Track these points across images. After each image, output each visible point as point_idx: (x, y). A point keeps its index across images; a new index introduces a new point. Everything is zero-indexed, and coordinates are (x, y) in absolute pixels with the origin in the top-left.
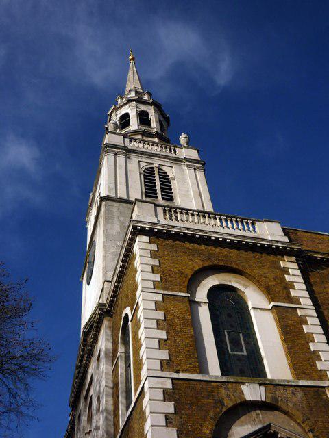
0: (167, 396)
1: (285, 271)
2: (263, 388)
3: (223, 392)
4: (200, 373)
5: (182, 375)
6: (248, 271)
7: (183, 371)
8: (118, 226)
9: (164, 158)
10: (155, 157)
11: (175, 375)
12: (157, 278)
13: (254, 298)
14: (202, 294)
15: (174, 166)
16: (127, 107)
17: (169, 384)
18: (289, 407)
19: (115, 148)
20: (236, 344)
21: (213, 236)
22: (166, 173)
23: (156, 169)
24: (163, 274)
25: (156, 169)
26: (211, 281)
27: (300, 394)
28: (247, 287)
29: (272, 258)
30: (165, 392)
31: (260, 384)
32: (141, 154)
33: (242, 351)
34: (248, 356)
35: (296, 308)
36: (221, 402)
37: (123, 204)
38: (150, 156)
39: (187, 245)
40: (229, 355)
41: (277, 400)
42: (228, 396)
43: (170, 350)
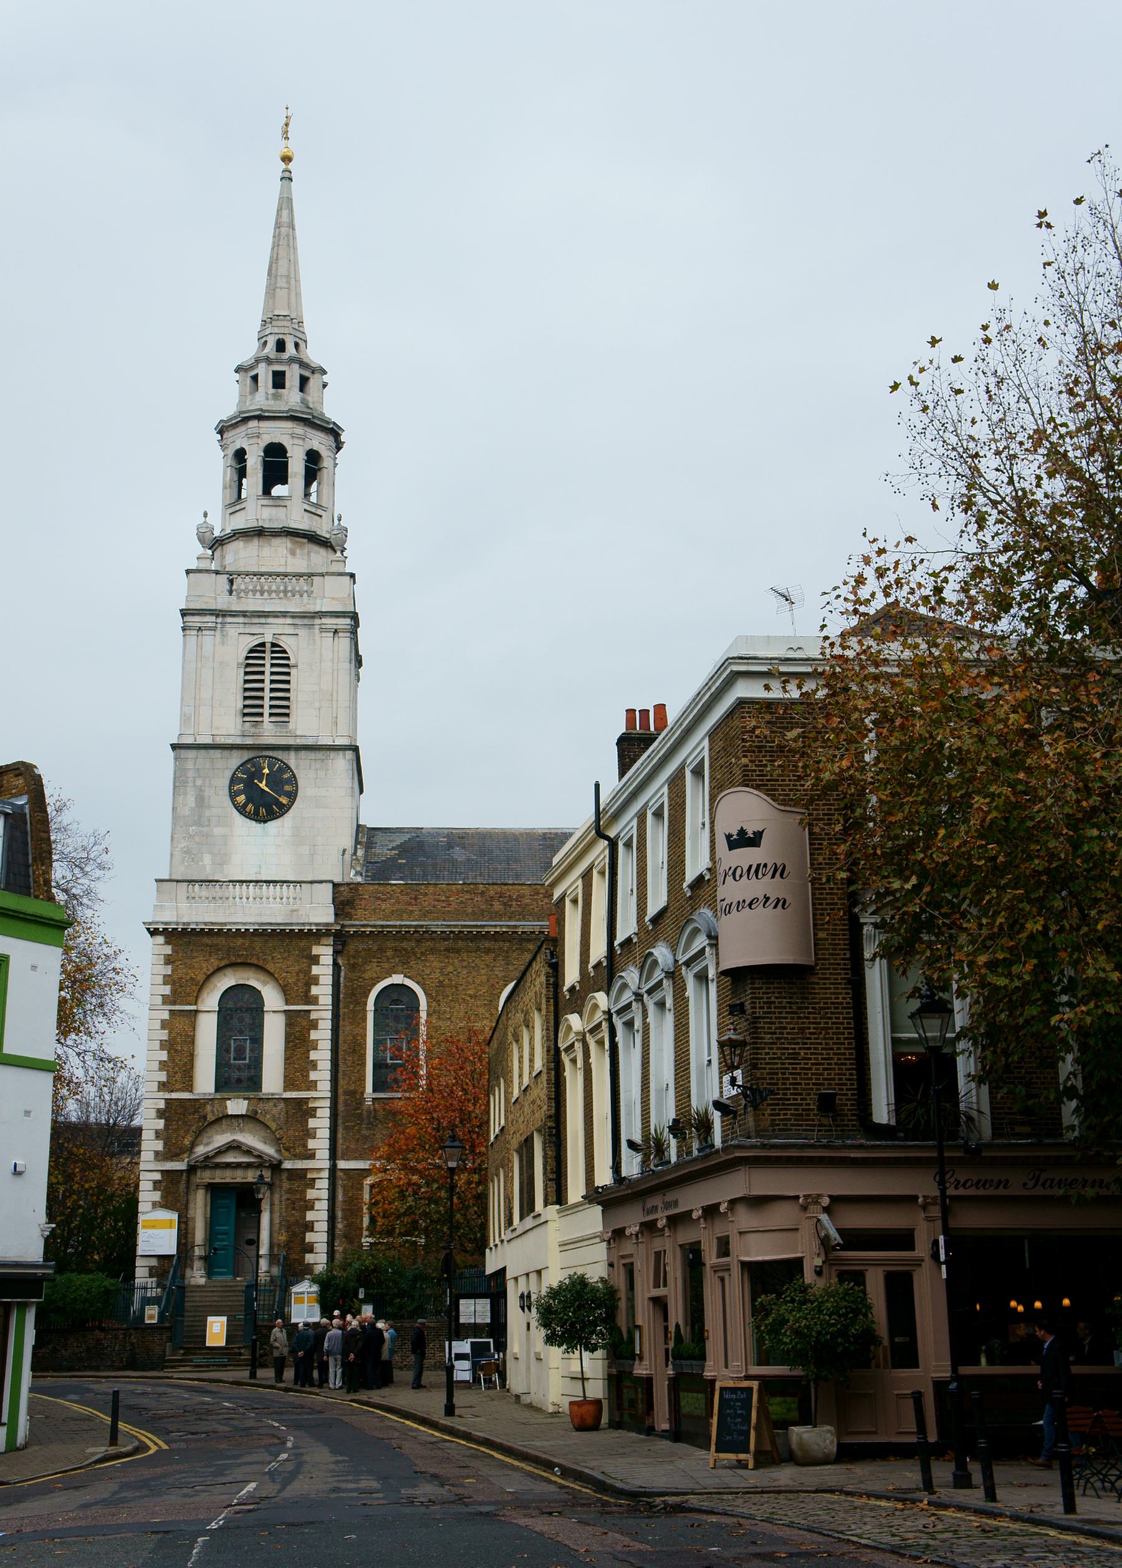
0: (160, 1114)
1: (315, 960)
2: (246, 1102)
3: (209, 1108)
4: (191, 1091)
5: (174, 1095)
6: (270, 967)
7: (177, 1091)
8: (193, 799)
9: (285, 617)
10: (267, 616)
11: (168, 1096)
12: (167, 990)
13: (272, 998)
14: (211, 1000)
15: (302, 632)
16: (242, 429)
17: (162, 1105)
18: (267, 1119)
19: (199, 614)
20: (240, 1053)
21: (234, 928)
22: (285, 652)
23: (268, 646)
24: (173, 983)
25: (268, 646)
26: (227, 981)
27: (282, 1105)
28: (265, 983)
29: (303, 944)
30: (158, 1110)
31: (245, 1099)
32: (245, 616)
33: (244, 1059)
34: (249, 1066)
35: (309, 1011)
36: (205, 1117)
37: (203, 752)
38: (259, 616)
39: (206, 940)
40: (230, 1066)
41: (256, 1112)
42: (213, 1112)
43: (168, 1071)
